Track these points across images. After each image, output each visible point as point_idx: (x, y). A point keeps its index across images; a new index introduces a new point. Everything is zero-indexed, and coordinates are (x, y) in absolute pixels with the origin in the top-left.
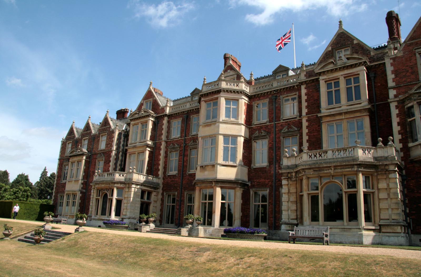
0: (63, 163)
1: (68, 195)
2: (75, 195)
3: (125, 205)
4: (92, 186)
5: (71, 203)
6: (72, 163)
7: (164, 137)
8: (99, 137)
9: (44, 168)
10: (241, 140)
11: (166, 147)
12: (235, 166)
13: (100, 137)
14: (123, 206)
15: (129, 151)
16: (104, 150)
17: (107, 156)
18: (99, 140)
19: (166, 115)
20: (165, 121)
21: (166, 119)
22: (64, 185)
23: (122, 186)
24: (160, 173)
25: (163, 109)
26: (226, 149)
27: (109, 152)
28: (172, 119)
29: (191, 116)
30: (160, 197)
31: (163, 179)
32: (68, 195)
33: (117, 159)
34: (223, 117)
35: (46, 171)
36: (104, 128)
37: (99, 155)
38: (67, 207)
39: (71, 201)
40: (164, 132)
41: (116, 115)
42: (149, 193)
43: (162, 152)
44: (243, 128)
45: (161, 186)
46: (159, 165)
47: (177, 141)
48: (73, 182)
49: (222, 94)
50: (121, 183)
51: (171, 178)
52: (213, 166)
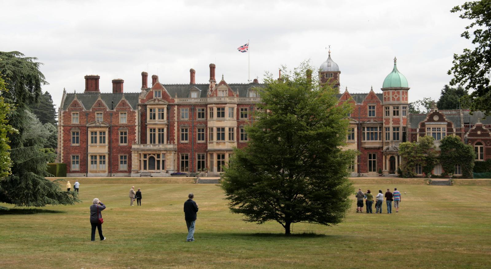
0: (70, 129)
1: (94, 157)
3: (168, 163)
4: (131, 152)
7: (176, 119)
8: (117, 113)
10: (235, 129)
11: (178, 125)
12: (234, 143)
13: (118, 114)
14: (166, 164)
16: (126, 124)
17: (131, 129)
18: (118, 116)
19: (177, 105)
20: (176, 108)
23: (165, 152)
24: (176, 141)
27: (133, 126)
28: (180, 107)
29: (197, 108)
31: (178, 145)
36: (123, 108)
37: (121, 128)
38: (92, 165)
39: (98, 159)
40: (176, 115)
41: (85, 79)
43: (176, 128)
44: (236, 122)
46: (174, 136)
47: (186, 122)
48: (98, 146)
49: (227, 105)
51: (183, 145)
52: (225, 143)
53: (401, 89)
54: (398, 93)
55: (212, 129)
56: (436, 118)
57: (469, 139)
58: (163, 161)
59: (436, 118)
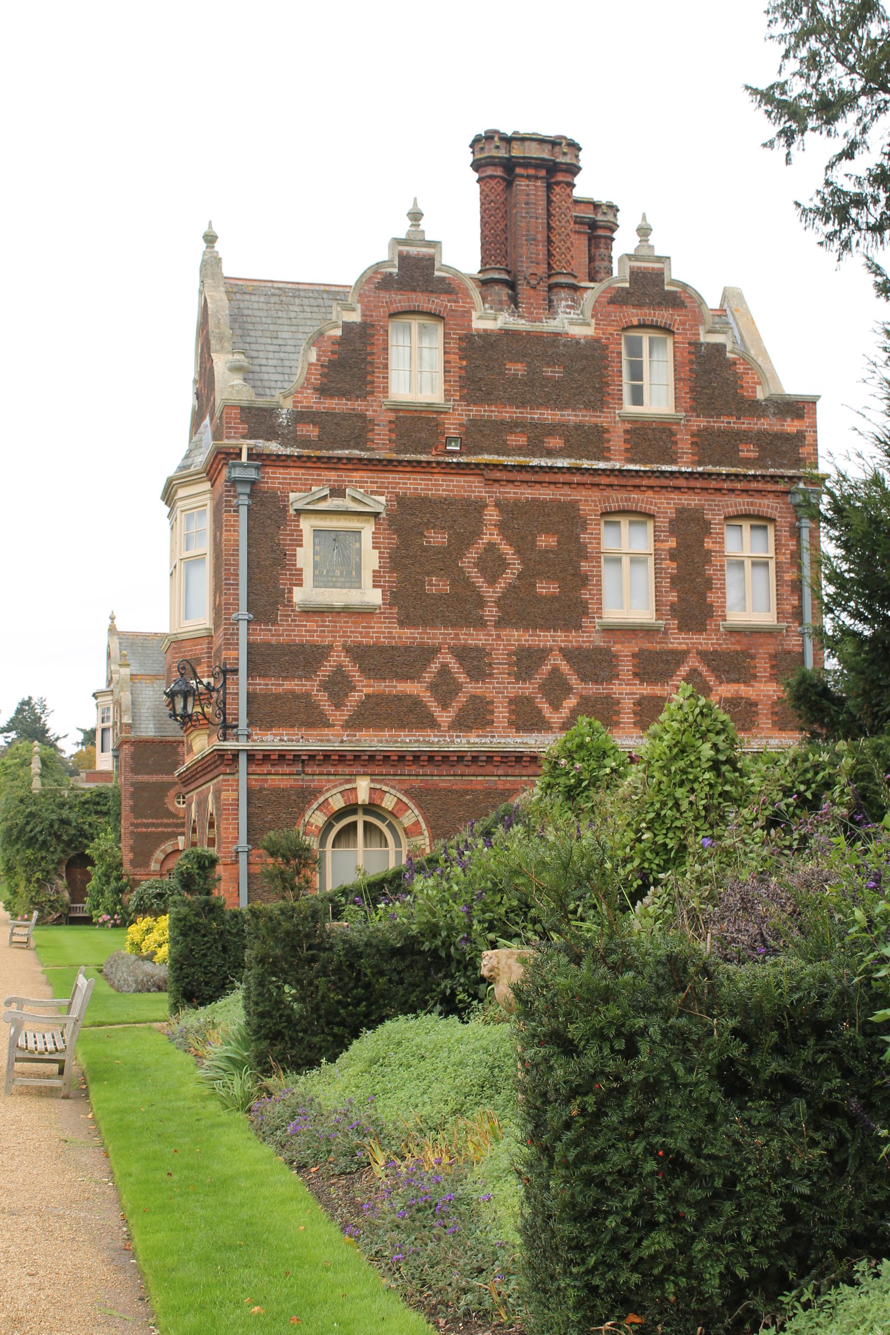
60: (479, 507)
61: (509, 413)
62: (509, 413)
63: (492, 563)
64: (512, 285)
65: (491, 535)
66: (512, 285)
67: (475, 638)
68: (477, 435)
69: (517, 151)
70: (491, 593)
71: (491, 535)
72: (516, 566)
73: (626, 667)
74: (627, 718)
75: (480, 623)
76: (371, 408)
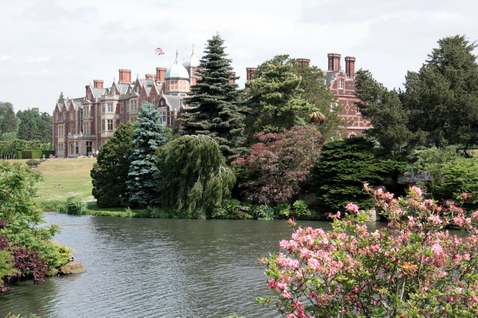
1: (60, 145)
2: (62, 145)
5: (61, 149)
6: (60, 127)
9: (60, 95)
10: (114, 121)
15: (84, 121)
21: (96, 105)
22: (57, 140)
25: (95, 99)
26: (109, 125)
30: (97, 143)
32: (60, 145)
33: (79, 125)
34: (107, 111)
35: (63, 97)
42: (91, 143)
45: (97, 138)
49: (106, 101)
50: (77, 139)
53: (170, 79)
54: (169, 82)
55: (104, 121)
56: (162, 104)
57: (177, 122)
58: (77, 148)
59: (162, 104)
60: (346, 101)
61: (349, 90)
62: (349, 90)
63: (347, 108)
64: (349, 75)
65: (347, 104)
66: (349, 75)
67: (346, 116)
68: (347, 93)
69: (351, 60)
70: (347, 111)
71: (347, 104)
72: (349, 108)
73: (359, 119)
74: (359, 125)
75: (346, 114)
76: (337, 90)
